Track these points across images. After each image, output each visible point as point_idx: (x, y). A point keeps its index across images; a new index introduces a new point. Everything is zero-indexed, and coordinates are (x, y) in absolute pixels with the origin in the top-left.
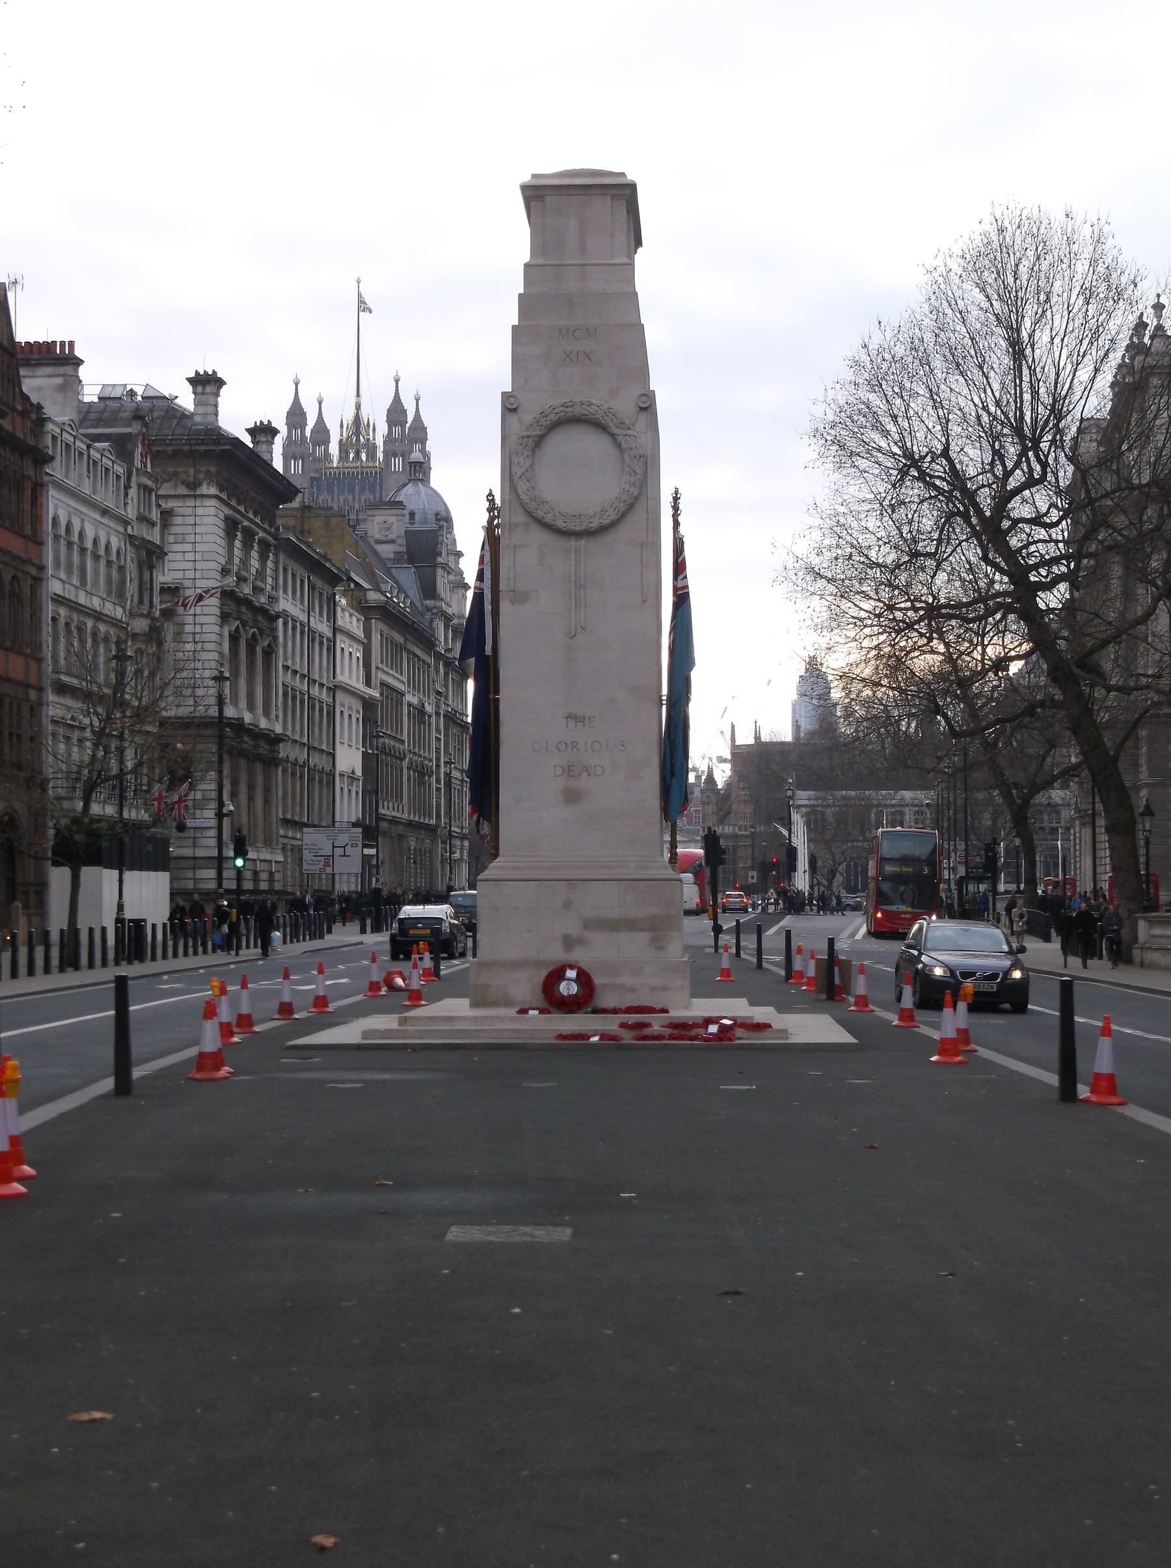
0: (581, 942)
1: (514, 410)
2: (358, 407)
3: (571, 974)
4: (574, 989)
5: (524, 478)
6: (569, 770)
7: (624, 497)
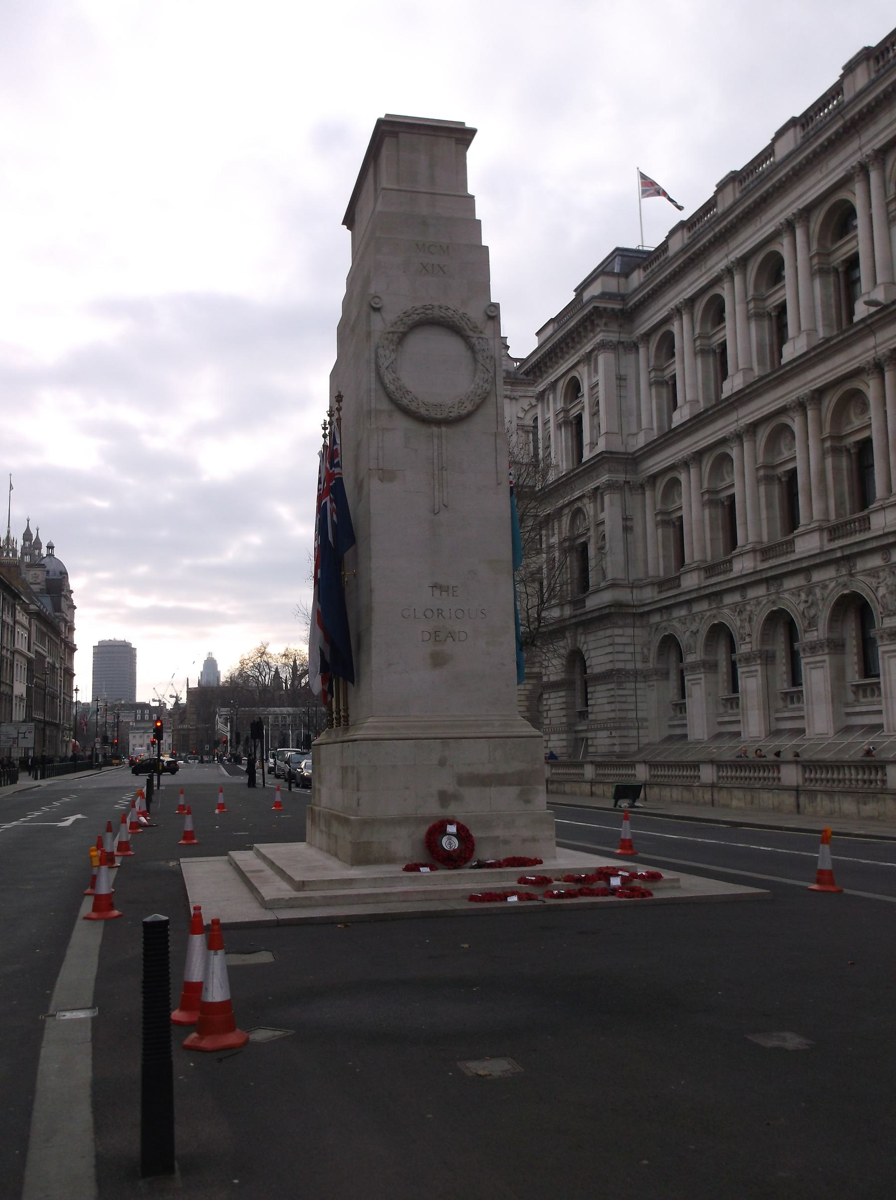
0: (456, 797)
1: (377, 310)
2: (9, 532)
3: (452, 829)
4: (456, 843)
5: (390, 369)
6: (435, 635)
7: (479, 392)
